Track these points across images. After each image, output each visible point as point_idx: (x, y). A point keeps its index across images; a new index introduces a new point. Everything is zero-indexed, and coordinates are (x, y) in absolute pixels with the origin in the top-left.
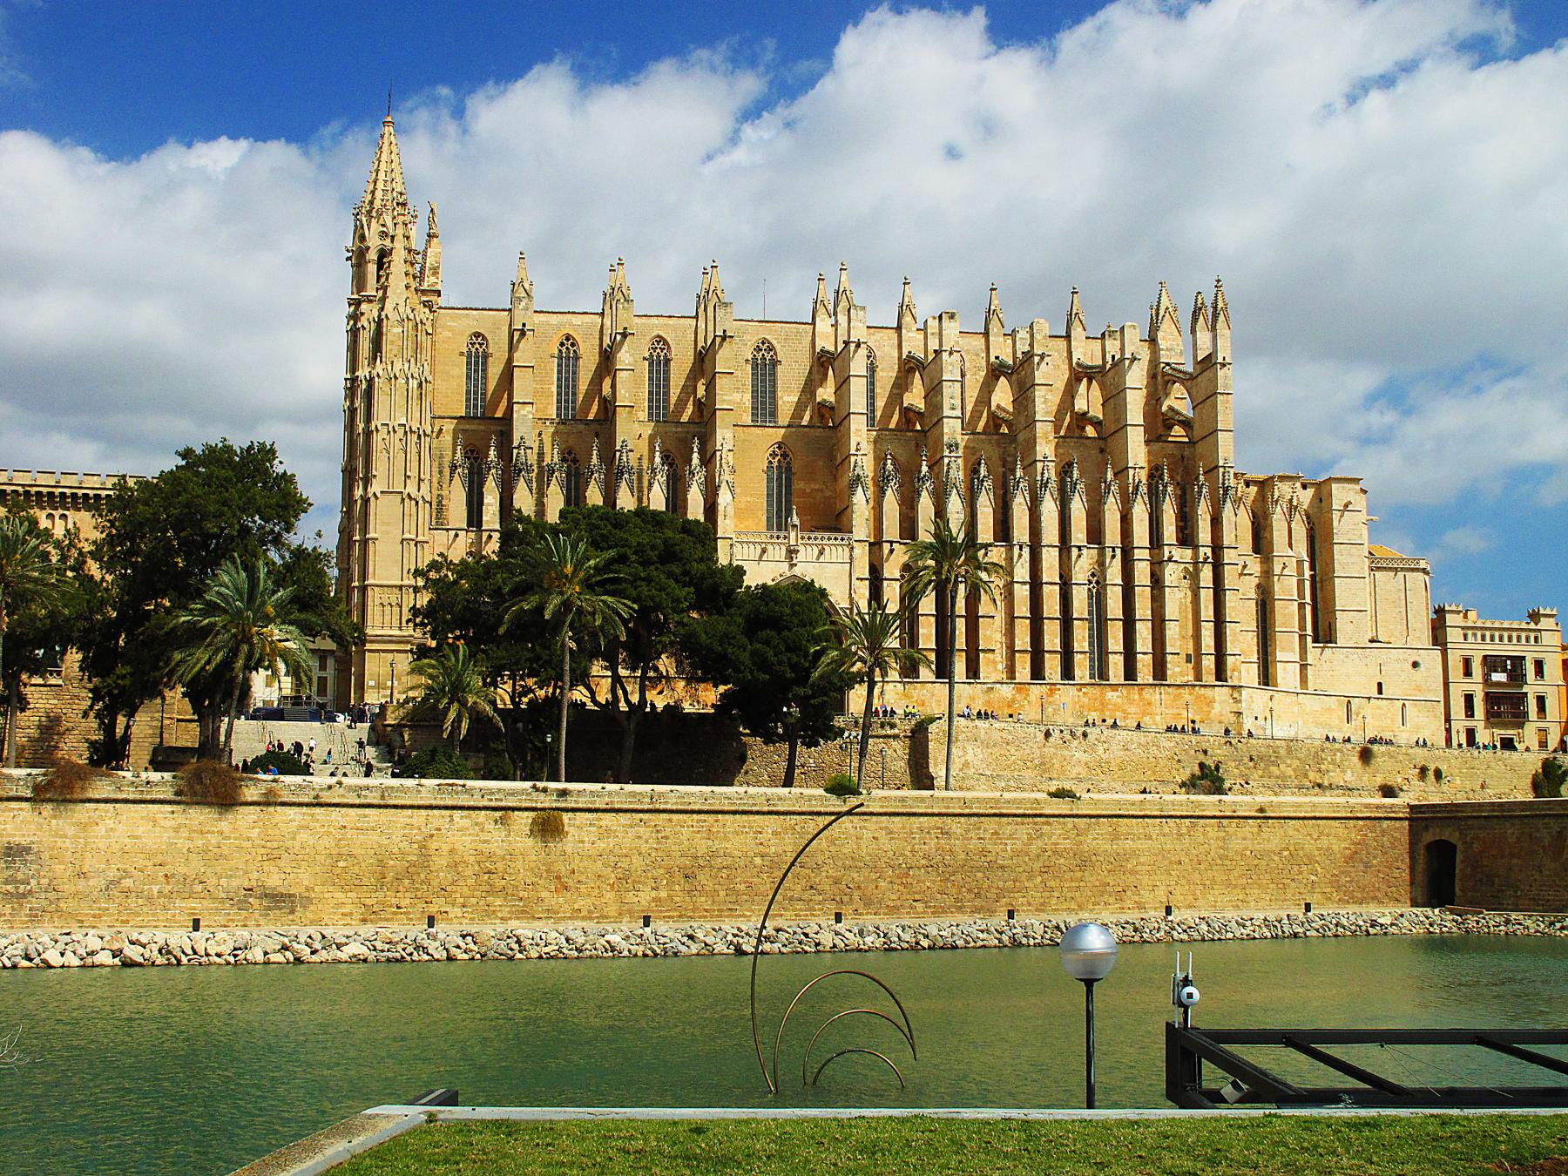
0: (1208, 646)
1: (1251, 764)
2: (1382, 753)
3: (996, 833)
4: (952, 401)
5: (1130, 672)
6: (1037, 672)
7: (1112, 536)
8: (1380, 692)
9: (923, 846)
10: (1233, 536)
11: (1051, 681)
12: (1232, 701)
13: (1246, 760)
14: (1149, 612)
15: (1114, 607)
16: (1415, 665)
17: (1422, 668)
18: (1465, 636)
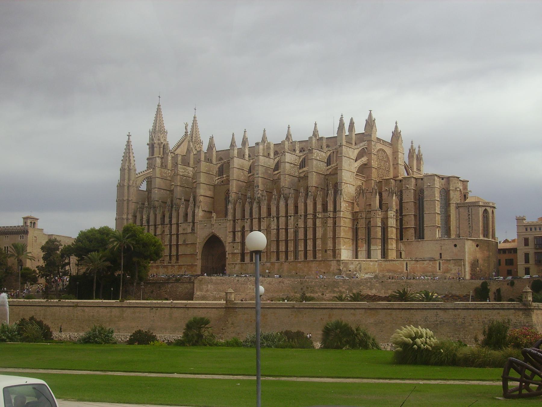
0: (329, 246)
1: (325, 288)
2: (393, 282)
3: (98, 311)
4: (257, 172)
5: (306, 256)
6: (278, 259)
7: (301, 211)
8: (441, 258)
9: (77, 314)
10: (340, 207)
11: (282, 261)
12: (337, 265)
13: (323, 286)
14: (312, 236)
15: (301, 236)
16: (455, 246)
17: (458, 246)
18: (526, 230)
